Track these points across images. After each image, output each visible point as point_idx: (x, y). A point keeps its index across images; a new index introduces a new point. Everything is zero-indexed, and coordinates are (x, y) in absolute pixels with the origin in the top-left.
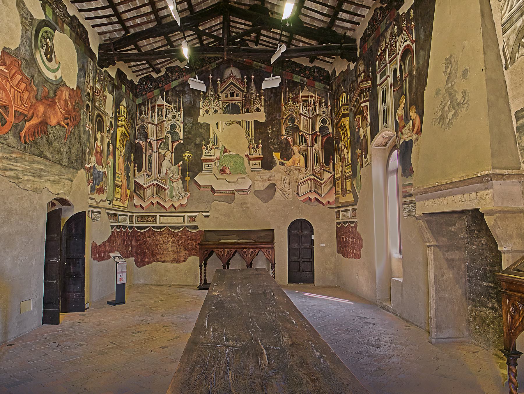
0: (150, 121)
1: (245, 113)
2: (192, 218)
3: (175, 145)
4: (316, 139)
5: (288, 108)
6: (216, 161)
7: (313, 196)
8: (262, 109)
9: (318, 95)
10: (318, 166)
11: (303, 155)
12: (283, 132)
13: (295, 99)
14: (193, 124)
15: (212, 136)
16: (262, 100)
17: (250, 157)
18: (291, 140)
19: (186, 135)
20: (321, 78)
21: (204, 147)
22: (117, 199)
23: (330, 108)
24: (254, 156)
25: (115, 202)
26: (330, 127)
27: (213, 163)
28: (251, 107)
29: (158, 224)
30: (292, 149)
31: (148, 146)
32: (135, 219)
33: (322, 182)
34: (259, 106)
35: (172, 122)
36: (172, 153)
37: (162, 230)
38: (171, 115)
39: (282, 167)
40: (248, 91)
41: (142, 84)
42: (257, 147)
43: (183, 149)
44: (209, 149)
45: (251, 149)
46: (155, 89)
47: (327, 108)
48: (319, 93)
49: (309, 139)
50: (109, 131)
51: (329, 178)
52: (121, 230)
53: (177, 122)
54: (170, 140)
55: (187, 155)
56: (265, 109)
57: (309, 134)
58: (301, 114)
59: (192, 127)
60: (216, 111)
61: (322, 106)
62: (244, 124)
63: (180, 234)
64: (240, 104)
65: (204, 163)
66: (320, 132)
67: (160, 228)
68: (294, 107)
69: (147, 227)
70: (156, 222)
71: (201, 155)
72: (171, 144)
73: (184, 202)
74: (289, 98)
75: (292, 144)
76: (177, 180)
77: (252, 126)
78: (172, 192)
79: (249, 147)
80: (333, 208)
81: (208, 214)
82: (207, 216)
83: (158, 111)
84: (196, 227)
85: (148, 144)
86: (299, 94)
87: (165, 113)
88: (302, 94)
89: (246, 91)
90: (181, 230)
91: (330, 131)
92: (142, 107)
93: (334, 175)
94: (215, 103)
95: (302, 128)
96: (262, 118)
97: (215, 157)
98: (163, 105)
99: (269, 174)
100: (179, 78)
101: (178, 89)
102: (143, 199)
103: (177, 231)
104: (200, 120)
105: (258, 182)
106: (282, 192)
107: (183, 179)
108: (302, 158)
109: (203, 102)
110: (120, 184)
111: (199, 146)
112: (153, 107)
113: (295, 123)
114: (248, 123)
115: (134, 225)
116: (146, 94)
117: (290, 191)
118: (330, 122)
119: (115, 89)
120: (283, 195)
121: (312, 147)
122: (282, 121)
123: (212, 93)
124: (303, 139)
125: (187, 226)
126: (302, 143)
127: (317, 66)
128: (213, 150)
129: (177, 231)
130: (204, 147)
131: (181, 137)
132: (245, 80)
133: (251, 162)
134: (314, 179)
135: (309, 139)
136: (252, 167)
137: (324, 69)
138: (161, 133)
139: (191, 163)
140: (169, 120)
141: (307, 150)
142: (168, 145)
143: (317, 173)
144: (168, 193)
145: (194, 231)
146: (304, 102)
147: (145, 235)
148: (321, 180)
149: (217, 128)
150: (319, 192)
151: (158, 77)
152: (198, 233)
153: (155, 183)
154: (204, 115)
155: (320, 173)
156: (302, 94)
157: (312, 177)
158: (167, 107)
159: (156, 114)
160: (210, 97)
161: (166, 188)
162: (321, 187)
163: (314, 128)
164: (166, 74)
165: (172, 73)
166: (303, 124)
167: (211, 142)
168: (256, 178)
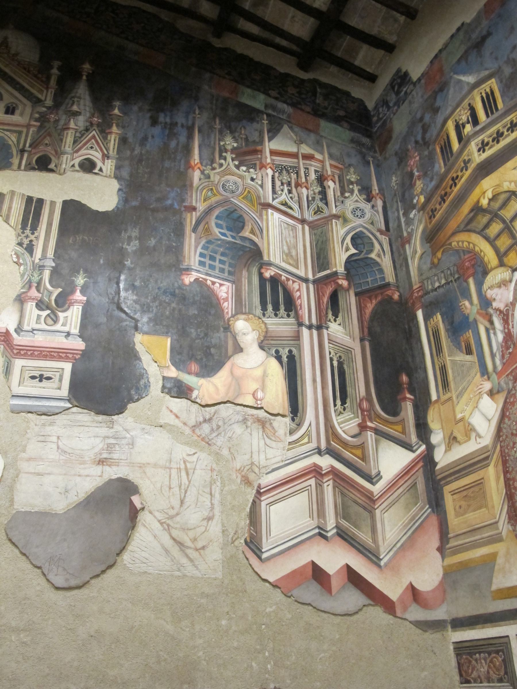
1: (30, 168)
4: (334, 298)
5: (215, 178)
7: (334, 559)
8: (109, 167)
9: (331, 156)
10: (348, 415)
11: (279, 358)
12: (192, 251)
13: (248, 155)
16: (113, 140)
17: (18, 340)
18: (224, 290)
20: (342, 113)
23: (380, 203)
24: (40, 340)
26: (386, 263)
28: (59, 154)
30: (227, 328)
33: (376, 489)
34: (96, 155)
39: (178, 404)
40: (57, 105)
42: (63, 302)
45: (30, 307)
47: (369, 199)
48: (335, 151)
49: (306, 298)
51: (407, 471)
56: (118, 168)
57: (306, 280)
58: (269, 206)
61: (352, 192)
62: (17, 208)
64: (14, 138)
66: (348, 276)
68: (241, 177)
74: (223, 150)
75: (228, 307)
77: (51, 221)
79: (21, 300)
80: (437, 625)
86: (261, 142)
88: (270, 145)
89: (49, 102)
91: (390, 277)
93: (428, 460)
95: (274, 252)
96: (102, 194)
99: (104, 431)
105: (40, 468)
106: (168, 528)
108: (276, 373)
113: (246, 233)
114: (34, 208)
117: (215, 528)
118: (387, 247)
120: (175, 551)
121: (319, 328)
122: (191, 219)
124: (276, 296)
126: (276, 308)
127: (324, 79)
132: (55, 71)
133: (19, 363)
134: (333, 471)
135: (306, 298)
136: (17, 390)
137: (347, 94)
141: (297, 337)
143: (345, 444)
146: (280, 169)
148: (369, 479)
150: (364, 536)
155: (362, 447)
156: (270, 145)
157: (326, 462)
162: (371, 512)
163: (321, 257)
166: (281, 240)
168: (33, 448)
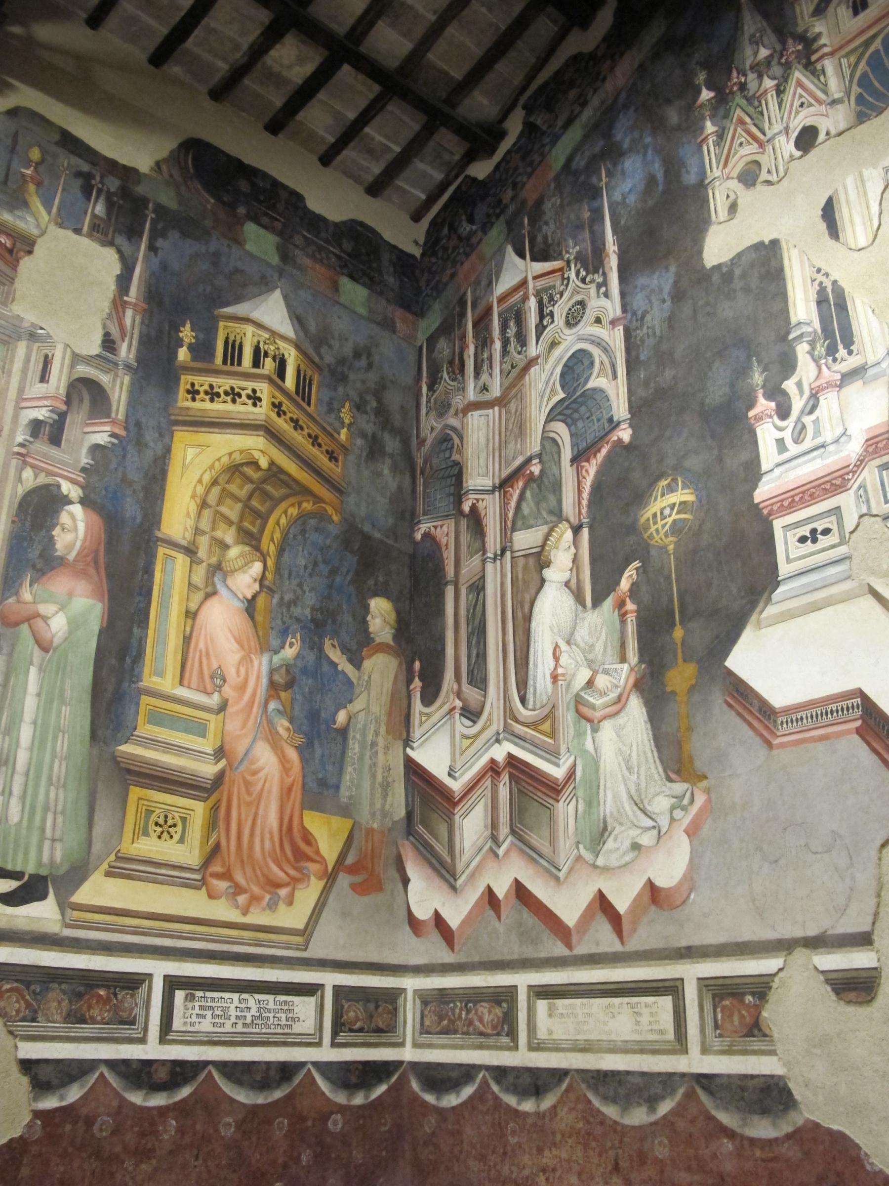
0: (471, 394)
2: (740, 1007)
3: (591, 469)
6: (870, 475)
14: (678, 296)
15: (802, 308)
19: (646, 383)
21: (764, 405)
22: (125, 868)
25: (99, 890)
27: (847, 501)
29: (521, 1058)
31: (465, 538)
32: (410, 1013)
35: (570, 342)
36: (576, 530)
37: (548, 1102)
38: (560, 310)
41: (437, 241)
43: (636, 476)
44: (797, 404)
46: (486, 227)
50: (52, 431)
52: (208, 1104)
53: (596, 330)
54: (567, 454)
55: (667, 507)
59: (671, 321)
60: (807, 139)
63: (661, 1150)
65: (778, 525)
67: (535, 1082)
69: (467, 1072)
70: (513, 1034)
71: (752, 472)
72: (568, 472)
73: (669, 867)
76: (620, 702)
78: (592, 802)
81: (860, 959)
82: (856, 987)
83: (504, 327)
84: (772, 1095)
85: (464, 522)
87: (532, 319)
90: (665, 1108)
92: (442, 344)
94: (788, 97)
97: (854, 448)
98: (524, 283)
100: (584, 104)
101: (580, 162)
102: (445, 871)
103: (638, 1117)
104: (719, 246)
107: (651, 686)
109: (720, 136)
110: (208, 769)
111: (730, 426)
112: (482, 322)
115: (408, 1054)
116: (453, 276)
119: (125, 211)
123: (764, 53)
125: (705, 1080)
128: (829, 402)
129: (638, 1117)
130: (764, 405)
131: (620, 408)
138: (521, 429)
139: (690, 557)
140: (554, 344)
142: (557, 487)
144: (566, 811)
145: (763, 1129)
147: (457, 1133)
149: (833, 230)
151: (497, 167)
152: (792, 1152)
153: (499, 753)
154: (733, 208)
158: (540, 284)
159: (498, 345)
160: (752, 85)
161: (558, 772)
164: (530, 129)
165: (549, 106)
167: (802, 349)
